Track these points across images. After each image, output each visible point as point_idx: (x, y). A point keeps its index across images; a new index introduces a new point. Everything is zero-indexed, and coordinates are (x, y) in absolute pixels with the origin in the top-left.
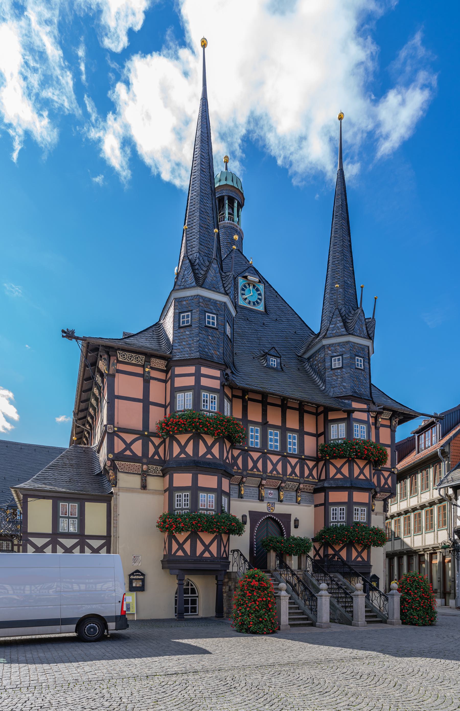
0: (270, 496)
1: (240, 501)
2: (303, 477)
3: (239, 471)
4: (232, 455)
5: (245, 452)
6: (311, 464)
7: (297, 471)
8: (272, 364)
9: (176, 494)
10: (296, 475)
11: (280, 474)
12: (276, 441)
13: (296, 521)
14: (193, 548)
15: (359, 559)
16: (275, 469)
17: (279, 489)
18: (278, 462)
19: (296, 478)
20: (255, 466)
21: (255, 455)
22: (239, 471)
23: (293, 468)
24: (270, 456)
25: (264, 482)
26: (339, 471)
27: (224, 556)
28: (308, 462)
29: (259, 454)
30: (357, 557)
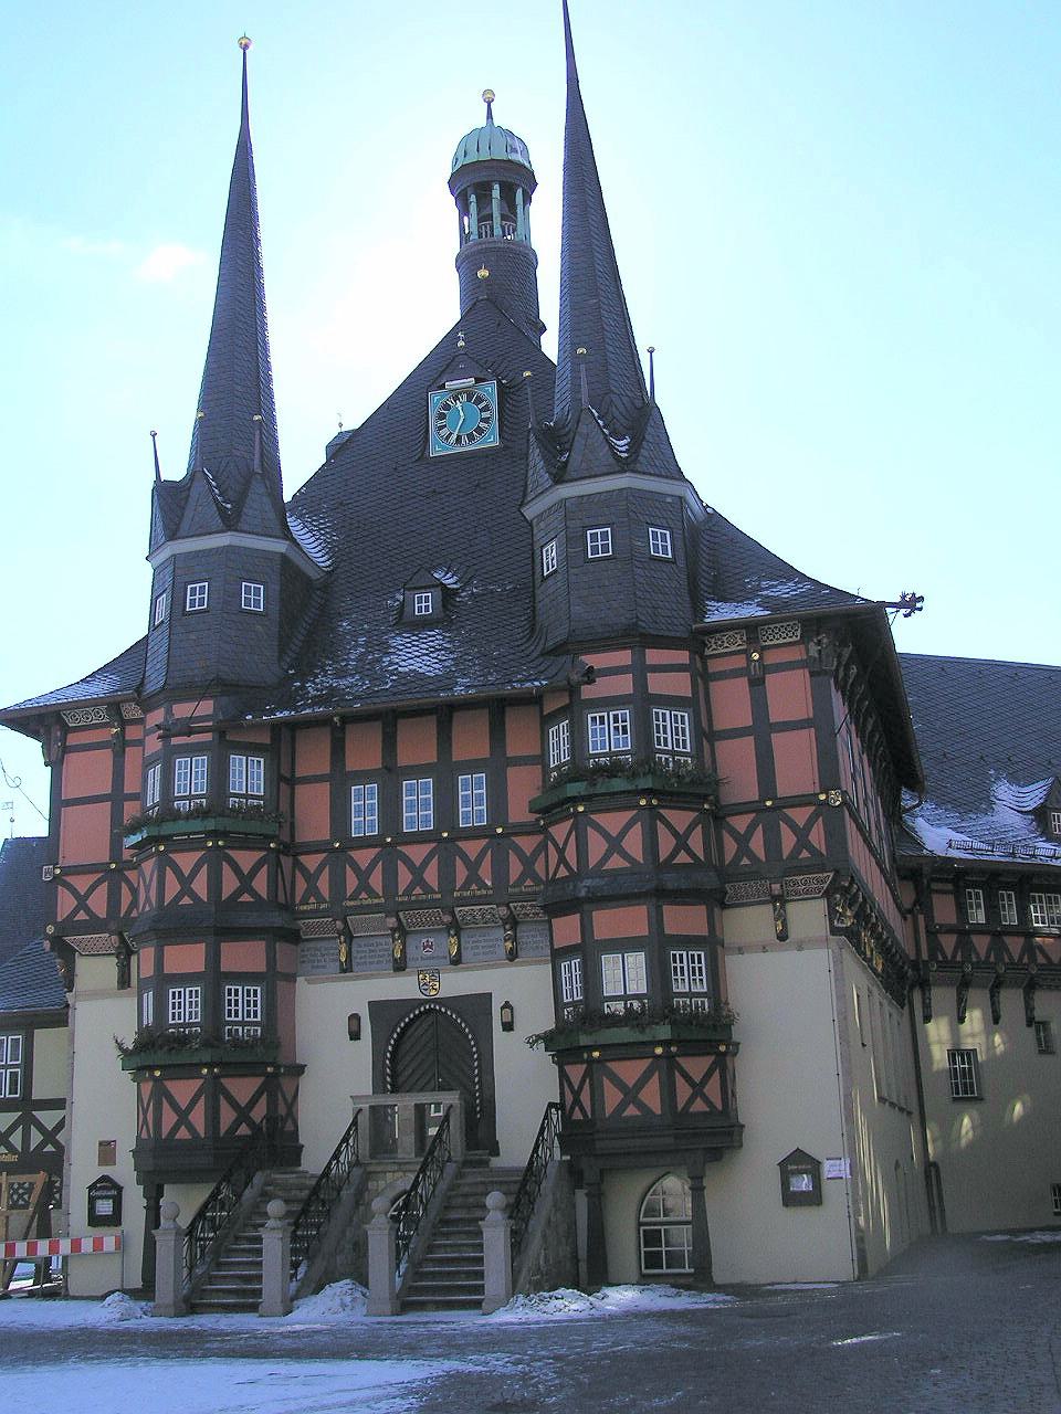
1: (346, 979)
6: (527, 844)
9: (171, 991)
10: (483, 886)
15: (631, 1111)
16: (418, 879)
18: (426, 862)
20: (364, 886)
21: (363, 857)
23: (473, 867)
26: (562, 860)
27: (244, 1130)
30: (623, 1106)
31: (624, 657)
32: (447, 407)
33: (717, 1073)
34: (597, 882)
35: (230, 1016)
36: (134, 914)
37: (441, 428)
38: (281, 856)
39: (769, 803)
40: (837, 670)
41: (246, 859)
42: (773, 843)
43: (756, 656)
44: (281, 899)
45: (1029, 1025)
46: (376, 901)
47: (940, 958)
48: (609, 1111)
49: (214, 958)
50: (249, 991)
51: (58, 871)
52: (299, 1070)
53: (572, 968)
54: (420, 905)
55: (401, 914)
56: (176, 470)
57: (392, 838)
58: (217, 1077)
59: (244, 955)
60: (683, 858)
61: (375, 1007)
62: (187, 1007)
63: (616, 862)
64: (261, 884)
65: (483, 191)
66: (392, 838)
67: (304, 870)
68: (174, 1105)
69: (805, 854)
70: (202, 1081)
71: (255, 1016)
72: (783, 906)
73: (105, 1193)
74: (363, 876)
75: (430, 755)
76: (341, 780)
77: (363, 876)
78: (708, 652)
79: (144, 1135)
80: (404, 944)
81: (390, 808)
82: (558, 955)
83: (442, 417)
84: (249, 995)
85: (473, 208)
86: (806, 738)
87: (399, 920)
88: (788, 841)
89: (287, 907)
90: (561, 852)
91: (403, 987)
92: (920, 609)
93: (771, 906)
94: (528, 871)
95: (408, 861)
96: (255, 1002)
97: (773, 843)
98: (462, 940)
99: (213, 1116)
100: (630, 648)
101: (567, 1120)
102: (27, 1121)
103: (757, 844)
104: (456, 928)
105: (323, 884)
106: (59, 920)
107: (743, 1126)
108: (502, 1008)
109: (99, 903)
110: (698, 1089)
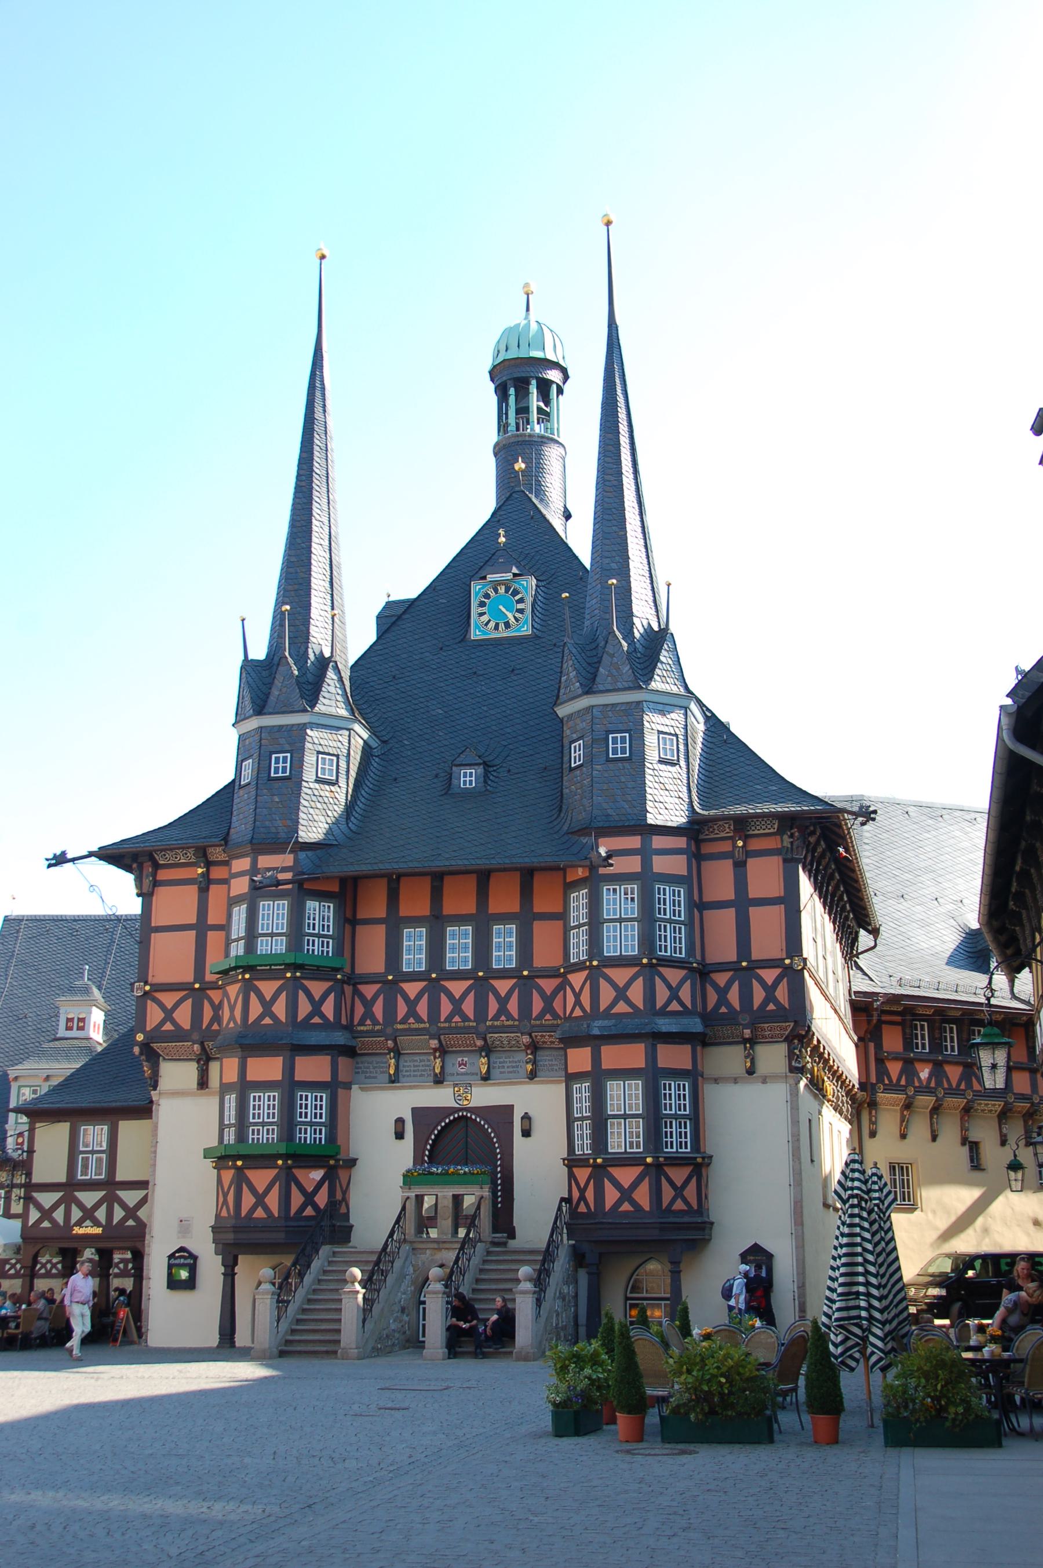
2: (531, 1018)
3: (378, 1027)
6: (548, 985)
7: (513, 1006)
8: (465, 781)
10: (509, 1017)
11: (469, 1020)
15: (626, 1207)
16: (457, 1010)
19: (510, 1023)
21: (412, 989)
22: (378, 1027)
23: (503, 1001)
24: (448, 984)
27: (309, 1211)
28: (541, 982)
29: (421, 985)
30: (619, 1203)
31: (634, 842)
32: (487, 596)
33: (694, 1180)
34: (606, 1023)
35: (301, 1117)
36: (215, 1027)
37: (481, 614)
38: (345, 986)
39: (744, 964)
40: (805, 858)
41: (317, 988)
42: (746, 996)
43: (740, 843)
44: (344, 1022)
45: (963, 1144)
46: (422, 1026)
47: (887, 1082)
48: (608, 1206)
49: (289, 1069)
50: (316, 1097)
51: (147, 988)
52: (352, 1162)
53: (582, 1091)
54: (458, 1030)
55: (442, 1037)
56: (259, 652)
57: (436, 976)
58: (290, 1168)
59: (313, 1068)
60: (675, 1006)
61: (414, 1110)
62: (265, 1106)
63: (622, 1007)
64: (328, 1009)
65: (522, 386)
66: (436, 976)
67: (362, 997)
68: (253, 1190)
69: (771, 1007)
70: (277, 1171)
71: (321, 1118)
72: (751, 1048)
73: (182, 1261)
74: (412, 1004)
75: (470, 907)
76: (395, 925)
77: (412, 1004)
78: (701, 837)
79: (224, 1213)
80: (443, 1061)
81: (436, 949)
82: (571, 1078)
83: (482, 604)
84: (316, 1100)
85: (512, 400)
86: (777, 912)
87: (440, 1041)
88: (759, 995)
89: (349, 1028)
90: (577, 996)
91: (442, 1097)
92: (874, 819)
93: (742, 1046)
94: (548, 1008)
95: (450, 995)
96: (321, 1106)
97: (746, 996)
98: (491, 1060)
99: (285, 1199)
100: (641, 835)
101: (574, 1213)
102: (111, 1200)
103: (734, 996)
104: (487, 1050)
105: (378, 1009)
106: (148, 1029)
107: (712, 1223)
108: (522, 1118)
109: (183, 1016)
110: (679, 1191)
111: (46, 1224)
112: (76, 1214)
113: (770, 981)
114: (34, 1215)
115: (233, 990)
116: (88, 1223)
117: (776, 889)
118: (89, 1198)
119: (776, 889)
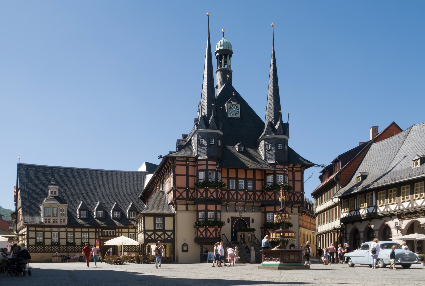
0: (240, 209)
4: (222, 193)
5: (228, 192)
6: (259, 194)
7: (252, 197)
10: (252, 200)
12: (242, 185)
13: (253, 220)
14: (206, 234)
16: (242, 197)
17: (244, 206)
20: (233, 197)
21: (233, 192)
23: (250, 196)
25: (237, 204)
26: (270, 197)
28: (257, 193)
61: (231, 217)
68: (210, 232)
74: (233, 196)
76: (228, 178)
77: (233, 196)
86: (300, 183)
88: (296, 198)
102: (164, 233)
103: (292, 198)
106: (176, 197)
109: (184, 195)
111: (149, 238)
112: (157, 236)
113: (298, 196)
114: (147, 236)
115: (202, 190)
116: (160, 238)
117: (299, 179)
118: (160, 233)
119: (300, 179)
